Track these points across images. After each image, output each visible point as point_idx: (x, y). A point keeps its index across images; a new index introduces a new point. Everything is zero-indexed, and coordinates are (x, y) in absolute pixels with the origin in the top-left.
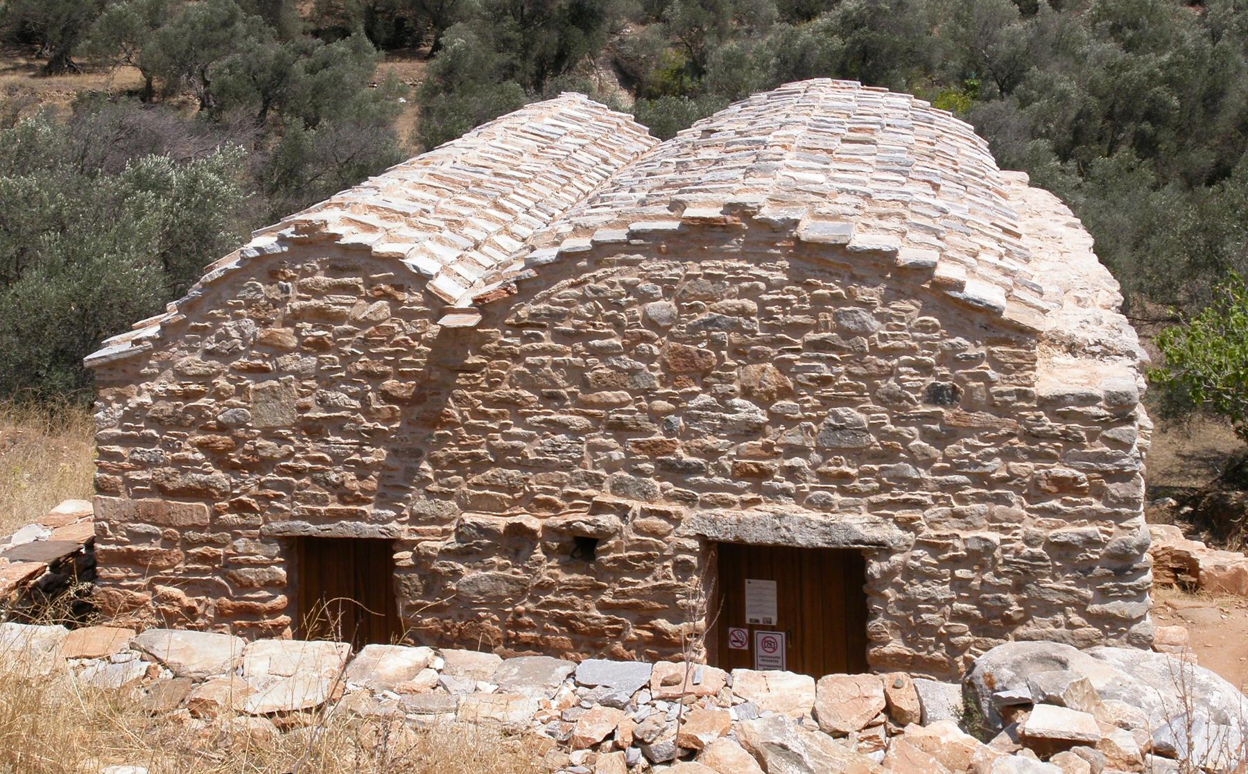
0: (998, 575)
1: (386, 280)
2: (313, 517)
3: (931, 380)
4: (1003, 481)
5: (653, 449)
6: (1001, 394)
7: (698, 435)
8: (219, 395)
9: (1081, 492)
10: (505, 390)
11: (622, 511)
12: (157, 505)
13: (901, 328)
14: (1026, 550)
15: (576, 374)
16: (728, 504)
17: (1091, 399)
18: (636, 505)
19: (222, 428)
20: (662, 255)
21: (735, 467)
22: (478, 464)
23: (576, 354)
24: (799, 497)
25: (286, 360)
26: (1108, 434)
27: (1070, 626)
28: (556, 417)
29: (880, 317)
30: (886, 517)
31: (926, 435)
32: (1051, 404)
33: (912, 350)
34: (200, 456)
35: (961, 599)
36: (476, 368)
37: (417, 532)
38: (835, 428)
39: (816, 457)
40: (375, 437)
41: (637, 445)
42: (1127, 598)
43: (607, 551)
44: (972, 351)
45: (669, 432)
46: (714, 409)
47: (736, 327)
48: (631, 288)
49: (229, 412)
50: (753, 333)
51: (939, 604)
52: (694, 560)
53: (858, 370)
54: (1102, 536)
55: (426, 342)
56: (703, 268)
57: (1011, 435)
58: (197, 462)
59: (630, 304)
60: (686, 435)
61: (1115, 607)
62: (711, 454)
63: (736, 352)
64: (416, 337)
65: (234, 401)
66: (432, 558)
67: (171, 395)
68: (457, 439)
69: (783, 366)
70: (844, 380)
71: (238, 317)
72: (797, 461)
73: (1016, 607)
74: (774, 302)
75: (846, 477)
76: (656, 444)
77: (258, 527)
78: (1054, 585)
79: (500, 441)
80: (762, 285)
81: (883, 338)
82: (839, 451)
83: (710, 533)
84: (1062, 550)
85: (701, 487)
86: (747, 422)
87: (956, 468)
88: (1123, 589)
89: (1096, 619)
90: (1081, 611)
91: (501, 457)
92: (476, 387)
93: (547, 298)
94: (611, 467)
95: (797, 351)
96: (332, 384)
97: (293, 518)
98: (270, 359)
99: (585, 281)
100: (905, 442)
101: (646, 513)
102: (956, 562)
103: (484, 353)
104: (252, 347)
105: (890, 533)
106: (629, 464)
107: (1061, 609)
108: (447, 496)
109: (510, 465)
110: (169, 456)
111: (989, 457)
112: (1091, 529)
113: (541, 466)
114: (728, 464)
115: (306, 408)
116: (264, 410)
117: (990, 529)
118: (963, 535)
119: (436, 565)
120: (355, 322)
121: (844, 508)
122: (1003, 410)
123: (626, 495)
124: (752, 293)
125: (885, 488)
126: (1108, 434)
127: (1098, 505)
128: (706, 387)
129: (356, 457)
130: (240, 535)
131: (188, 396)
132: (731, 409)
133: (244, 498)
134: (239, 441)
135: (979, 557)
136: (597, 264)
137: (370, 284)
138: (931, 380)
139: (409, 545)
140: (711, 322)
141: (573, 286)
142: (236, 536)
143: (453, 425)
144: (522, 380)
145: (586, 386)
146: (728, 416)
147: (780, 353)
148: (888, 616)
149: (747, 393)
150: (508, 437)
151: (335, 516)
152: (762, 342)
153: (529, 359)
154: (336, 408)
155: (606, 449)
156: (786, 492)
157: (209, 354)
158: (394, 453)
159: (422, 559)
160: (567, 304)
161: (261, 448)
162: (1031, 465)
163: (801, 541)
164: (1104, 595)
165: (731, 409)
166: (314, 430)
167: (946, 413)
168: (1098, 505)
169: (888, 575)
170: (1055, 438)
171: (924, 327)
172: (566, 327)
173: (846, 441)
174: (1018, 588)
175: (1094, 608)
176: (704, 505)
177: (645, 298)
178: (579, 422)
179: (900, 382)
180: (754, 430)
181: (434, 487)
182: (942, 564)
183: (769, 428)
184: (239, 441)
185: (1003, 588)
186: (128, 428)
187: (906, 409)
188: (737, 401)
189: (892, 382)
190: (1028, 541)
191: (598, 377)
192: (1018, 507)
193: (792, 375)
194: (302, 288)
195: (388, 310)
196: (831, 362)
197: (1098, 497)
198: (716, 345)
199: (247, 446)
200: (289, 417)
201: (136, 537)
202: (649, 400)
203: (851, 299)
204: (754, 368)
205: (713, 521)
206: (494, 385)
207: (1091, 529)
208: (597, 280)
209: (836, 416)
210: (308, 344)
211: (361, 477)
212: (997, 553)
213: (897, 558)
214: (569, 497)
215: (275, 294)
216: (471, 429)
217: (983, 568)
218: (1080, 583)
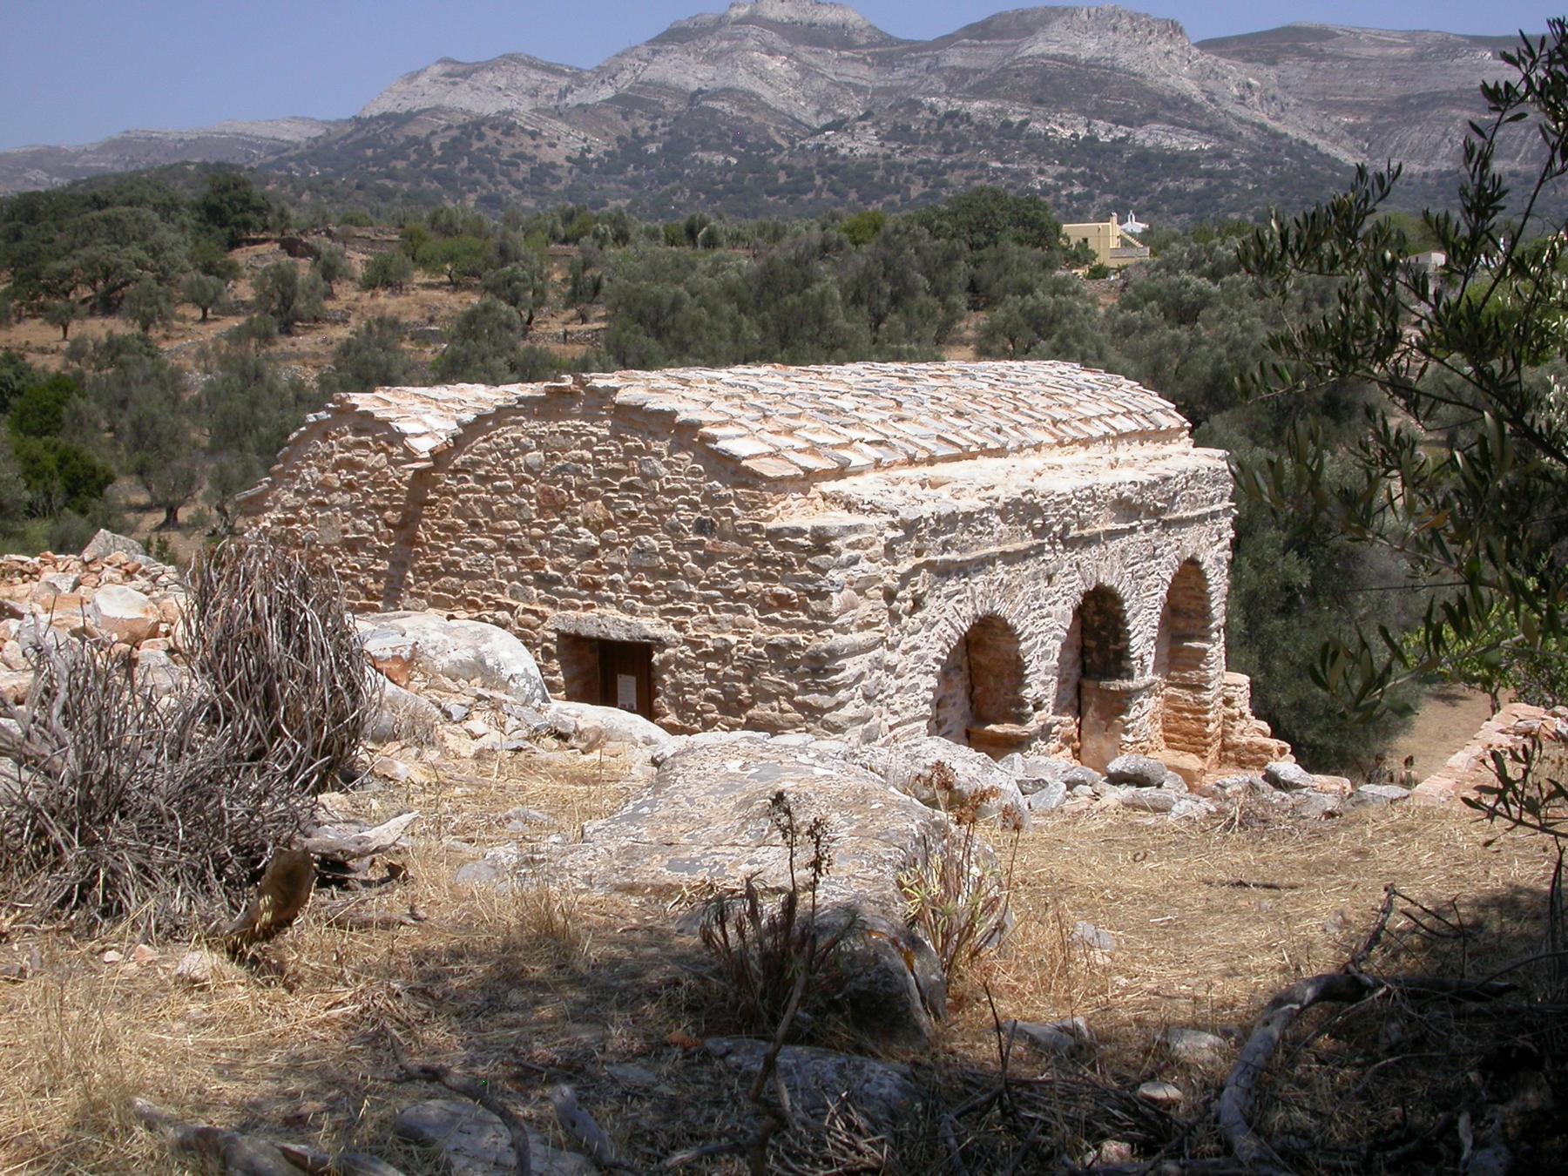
0: (734, 668)
1: (384, 438)
3: (698, 515)
4: (742, 596)
5: (533, 565)
6: (741, 526)
7: (559, 555)
8: (303, 522)
9: (793, 607)
10: (449, 519)
11: (511, 609)
13: (679, 473)
14: (753, 649)
15: (487, 506)
16: (576, 607)
17: (799, 532)
18: (522, 606)
20: (537, 417)
21: (580, 580)
22: (437, 574)
23: (488, 492)
24: (618, 604)
25: (334, 496)
26: (811, 560)
27: (782, 711)
28: (477, 539)
29: (668, 465)
30: (668, 621)
31: (696, 559)
32: (774, 535)
33: (686, 491)
35: (711, 686)
36: (433, 502)
38: (639, 552)
39: (627, 573)
40: (382, 553)
41: (523, 561)
42: (821, 692)
44: (723, 492)
45: (542, 553)
46: (567, 535)
47: (577, 472)
48: (517, 441)
50: (589, 477)
51: (698, 688)
52: (553, 647)
53: (652, 506)
54: (802, 642)
55: (405, 483)
57: (747, 560)
59: (517, 454)
60: (552, 555)
61: (813, 699)
62: (565, 569)
63: (581, 491)
64: (400, 479)
67: (279, 522)
69: (607, 502)
70: (645, 513)
71: (309, 466)
72: (616, 576)
73: (746, 694)
74: (601, 452)
75: (644, 590)
76: (534, 561)
78: (771, 678)
80: (594, 439)
82: (641, 569)
83: (561, 627)
85: (561, 595)
86: (585, 544)
87: (713, 586)
88: (818, 684)
89: (801, 707)
90: (790, 701)
91: (451, 568)
92: (433, 516)
93: (470, 451)
94: (510, 577)
95: (615, 491)
96: (358, 514)
98: (326, 496)
100: (682, 563)
101: (526, 611)
102: (707, 656)
105: (668, 632)
106: (518, 576)
107: (776, 697)
108: (421, 596)
109: (453, 575)
111: (734, 577)
112: (799, 637)
113: (469, 576)
114: (575, 577)
115: (345, 531)
116: (325, 533)
117: (734, 633)
118: (713, 636)
120: (368, 469)
121: (644, 613)
122: (744, 540)
123: (517, 599)
124: (587, 445)
125: (669, 599)
126: (811, 560)
127: (803, 618)
128: (563, 518)
131: (289, 522)
132: (576, 536)
135: (722, 653)
136: (499, 424)
137: (376, 441)
138: (698, 515)
140: (563, 468)
143: (421, 544)
144: (459, 512)
145: (494, 519)
148: (667, 696)
149: (586, 524)
150: (452, 554)
152: (594, 484)
155: (506, 564)
156: (609, 599)
157: (297, 492)
158: (392, 564)
162: (761, 584)
163: (614, 636)
164: (805, 689)
165: (576, 536)
166: (352, 547)
167: (708, 542)
168: (803, 618)
169: (665, 662)
170: (776, 563)
171: (693, 473)
173: (645, 561)
174: (747, 680)
175: (798, 698)
176: (563, 608)
177: (526, 450)
178: (490, 543)
180: (592, 552)
181: (414, 589)
182: (699, 657)
185: (737, 678)
187: (681, 537)
188: (580, 529)
190: (754, 643)
191: (499, 509)
192: (752, 615)
193: (613, 510)
194: (341, 445)
195: (385, 460)
196: (636, 499)
197: (805, 611)
198: (568, 486)
200: (336, 538)
203: (649, 451)
204: (590, 504)
206: (443, 515)
207: (799, 637)
208: (499, 436)
209: (641, 544)
211: (377, 582)
212: (734, 651)
213: (669, 651)
214: (486, 598)
216: (432, 547)
217: (725, 664)
218: (789, 679)
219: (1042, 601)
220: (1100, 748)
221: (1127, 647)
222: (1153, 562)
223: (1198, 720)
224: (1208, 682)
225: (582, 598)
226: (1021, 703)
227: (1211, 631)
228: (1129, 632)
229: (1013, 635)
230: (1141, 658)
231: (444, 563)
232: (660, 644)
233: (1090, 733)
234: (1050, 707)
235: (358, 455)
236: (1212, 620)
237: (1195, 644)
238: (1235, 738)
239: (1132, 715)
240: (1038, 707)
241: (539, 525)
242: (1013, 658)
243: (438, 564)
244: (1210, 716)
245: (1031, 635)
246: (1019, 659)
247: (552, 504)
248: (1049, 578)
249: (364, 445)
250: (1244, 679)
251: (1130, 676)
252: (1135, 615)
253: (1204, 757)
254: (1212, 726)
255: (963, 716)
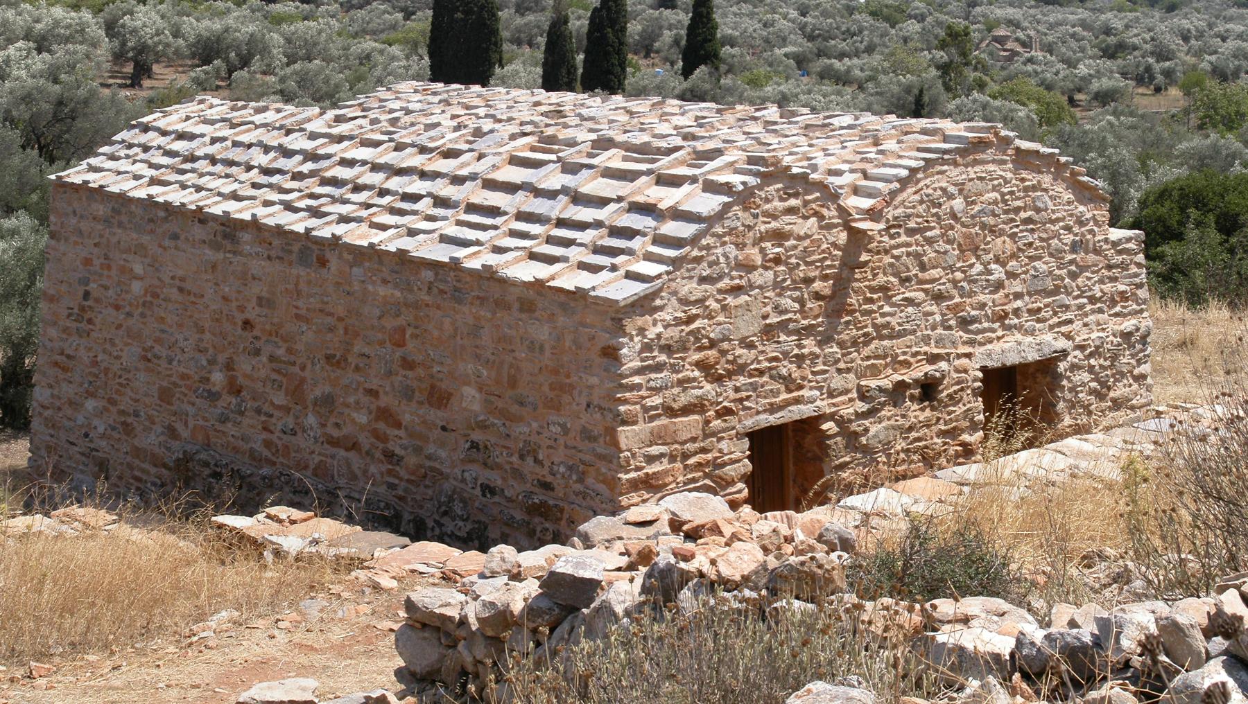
2: (773, 409)
5: (956, 309)
10: (881, 279)
12: (665, 426)
19: (713, 344)
22: (868, 339)
28: (907, 295)
33: (1063, 219)
34: (697, 373)
36: (866, 263)
37: (834, 405)
38: (1035, 277)
40: (809, 330)
43: (942, 391)
49: (718, 329)
56: (976, 173)
58: (694, 380)
62: (982, 306)
65: (721, 318)
66: (850, 421)
67: (678, 322)
68: (856, 323)
70: (1037, 243)
76: (957, 305)
77: (734, 428)
79: (880, 320)
81: (1053, 212)
83: (989, 364)
84: (1126, 336)
85: (979, 332)
95: (1017, 226)
97: (758, 413)
99: (922, 189)
103: (869, 251)
104: (732, 269)
105: (1062, 344)
110: (675, 377)
115: (765, 317)
119: (854, 427)
120: (799, 238)
122: (1097, 252)
129: (796, 351)
130: (723, 438)
133: (726, 404)
134: (723, 353)
139: (831, 417)
141: (916, 193)
142: (720, 439)
146: (990, 278)
147: (1011, 228)
149: (997, 260)
150: (883, 315)
151: (787, 404)
153: (895, 252)
154: (786, 311)
155: (932, 314)
159: (842, 422)
160: (914, 207)
161: (739, 357)
172: (912, 225)
176: (981, 344)
177: (951, 197)
179: (1060, 240)
180: (999, 285)
181: (842, 365)
183: (1007, 283)
184: (723, 353)
186: (647, 358)
189: (1056, 241)
196: (1032, 231)
199: (730, 357)
200: (756, 327)
201: (651, 459)
202: (953, 272)
205: (989, 355)
206: (875, 275)
209: (1035, 269)
210: (770, 260)
214: (915, 354)
215: (750, 221)
225: (994, 331)
231: (875, 326)
232: (1064, 353)
235: (786, 220)
241: (959, 269)
243: (870, 329)
247: (971, 248)
249: (791, 211)
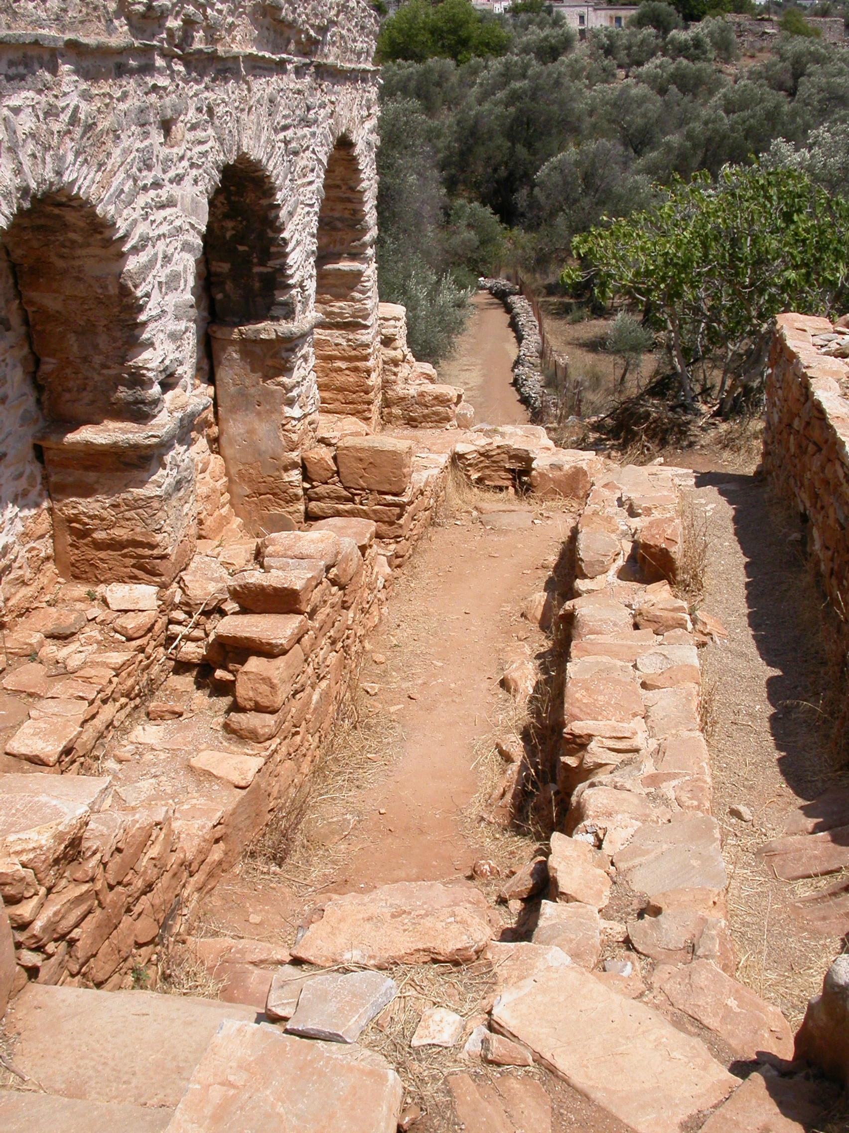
219: (157, 172)
220: (251, 432)
221: (283, 268)
222: (306, 130)
223: (356, 370)
224: (365, 317)
226: (138, 380)
227: (364, 246)
228: (285, 242)
229: (109, 243)
230: (302, 287)
233: (233, 410)
234: (187, 379)
236: (365, 231)
237: (345, 265)
238: (399, 389)
239: (297, 375)
240: (167, 384)
242: (113, 290)
244: (371, 363)
245: (145, 240)
246: (125, 292)
248: (166, 126)
250: (399, 310)
251: (289, 314)
252: (291, 214)
253: (367, 419)
254: (374, 375)
255: (25, 420)
